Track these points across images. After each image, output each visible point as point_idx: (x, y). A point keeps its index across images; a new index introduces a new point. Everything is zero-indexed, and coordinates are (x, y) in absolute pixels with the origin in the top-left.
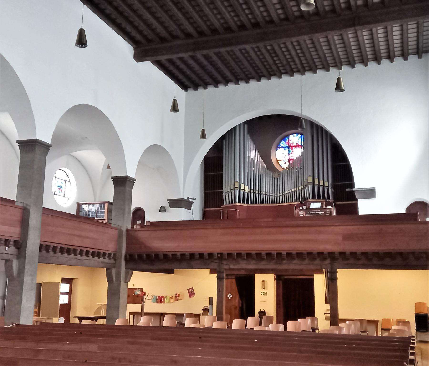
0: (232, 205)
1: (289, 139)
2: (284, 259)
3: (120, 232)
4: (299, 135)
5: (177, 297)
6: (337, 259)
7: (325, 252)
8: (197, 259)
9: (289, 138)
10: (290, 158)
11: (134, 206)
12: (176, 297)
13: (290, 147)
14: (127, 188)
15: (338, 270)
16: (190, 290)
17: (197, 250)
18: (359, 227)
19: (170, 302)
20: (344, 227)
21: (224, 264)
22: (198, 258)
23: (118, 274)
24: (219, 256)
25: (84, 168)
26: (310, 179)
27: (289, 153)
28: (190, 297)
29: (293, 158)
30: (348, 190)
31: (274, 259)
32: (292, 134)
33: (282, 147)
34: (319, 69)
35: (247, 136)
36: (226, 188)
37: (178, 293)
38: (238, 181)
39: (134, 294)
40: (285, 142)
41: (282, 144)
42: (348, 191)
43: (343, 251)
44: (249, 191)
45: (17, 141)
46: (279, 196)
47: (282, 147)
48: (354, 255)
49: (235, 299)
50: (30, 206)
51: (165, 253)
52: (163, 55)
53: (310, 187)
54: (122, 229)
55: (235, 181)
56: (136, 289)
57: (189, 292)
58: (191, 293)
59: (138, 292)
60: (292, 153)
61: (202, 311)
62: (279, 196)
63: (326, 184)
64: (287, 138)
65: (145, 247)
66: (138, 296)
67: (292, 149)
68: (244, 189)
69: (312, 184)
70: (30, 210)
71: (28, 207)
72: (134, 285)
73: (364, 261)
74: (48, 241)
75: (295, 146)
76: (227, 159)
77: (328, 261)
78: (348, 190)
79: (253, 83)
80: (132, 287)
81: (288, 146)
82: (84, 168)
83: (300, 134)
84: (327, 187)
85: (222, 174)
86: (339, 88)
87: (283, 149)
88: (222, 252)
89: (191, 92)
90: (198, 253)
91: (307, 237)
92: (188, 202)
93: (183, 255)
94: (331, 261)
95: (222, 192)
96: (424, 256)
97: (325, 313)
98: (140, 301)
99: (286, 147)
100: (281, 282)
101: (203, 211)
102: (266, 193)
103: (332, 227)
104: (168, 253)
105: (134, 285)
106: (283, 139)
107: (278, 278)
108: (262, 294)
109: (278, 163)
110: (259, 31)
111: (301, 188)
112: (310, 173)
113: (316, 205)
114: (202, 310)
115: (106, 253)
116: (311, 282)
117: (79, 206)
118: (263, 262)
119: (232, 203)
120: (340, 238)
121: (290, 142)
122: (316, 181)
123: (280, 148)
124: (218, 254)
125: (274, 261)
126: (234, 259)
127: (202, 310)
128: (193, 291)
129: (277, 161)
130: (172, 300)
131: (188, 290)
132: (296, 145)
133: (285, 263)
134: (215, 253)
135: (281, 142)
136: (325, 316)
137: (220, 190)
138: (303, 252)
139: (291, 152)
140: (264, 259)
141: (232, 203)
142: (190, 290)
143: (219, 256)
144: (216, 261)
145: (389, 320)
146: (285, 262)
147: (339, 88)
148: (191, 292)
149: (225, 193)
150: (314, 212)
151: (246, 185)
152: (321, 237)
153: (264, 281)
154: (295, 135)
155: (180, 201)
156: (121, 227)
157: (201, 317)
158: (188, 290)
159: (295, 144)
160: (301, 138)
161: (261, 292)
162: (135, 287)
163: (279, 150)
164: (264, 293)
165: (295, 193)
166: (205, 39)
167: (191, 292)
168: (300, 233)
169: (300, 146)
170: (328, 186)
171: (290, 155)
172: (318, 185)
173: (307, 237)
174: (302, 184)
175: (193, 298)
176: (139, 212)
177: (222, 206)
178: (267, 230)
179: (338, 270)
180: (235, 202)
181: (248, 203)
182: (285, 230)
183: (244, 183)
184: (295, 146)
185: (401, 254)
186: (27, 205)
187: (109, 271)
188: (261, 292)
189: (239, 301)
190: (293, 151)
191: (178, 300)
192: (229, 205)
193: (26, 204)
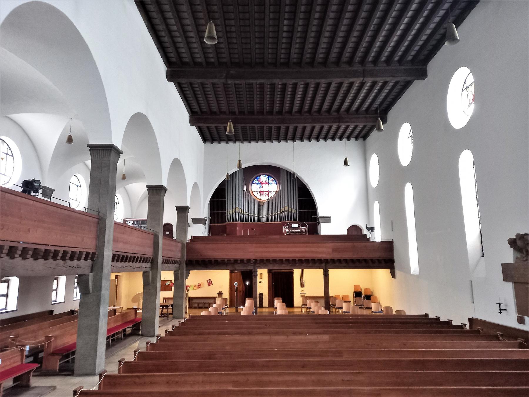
0: (230, 223)
1: (260, 178)
2: (297, 263)
3: (183, 244)
4: (267, 176)
5: (199, 286)
6: (329, 263)
7: (323, 259)
8: (239, 264)
9: (260, 177)
10: (261, 191)
11: (165, 222)
12: (198, 286)
13: (261, 183)
14: (187, 214)
15: (329, 269)
16: (209, 281)
17: (239, 257)
18: (342, 244)
19: (193, 289)
20: (333, 244)
21: (257, 266)
22: (239, 263)
23: (182, 274)
24: (254, 261)
25: (127, 192)
26: (286, 208)
27: (260, 187)
28: (209, 285)
29: (263, 191)
30: (313, 216)
31: (290, 263)
32: (262, 175)
33: (256, 183)
34: (298, 139)
35: (243, 176)
36: (229, 212)
37: (199, 283)
38: (238, 206)
39: (165, 285)
40: (258, 180)
41: (256, 181)
42: (313, 218)
43: (333, 259)
44: (244, 213)
45: (146, 186)
46: (264, 217)
47: (256, 183)
48: (339, 261)
49: (240, 286)
50: (159, 233)
51: (215, 259)
52: (213, 123)
53: (286, 213)
54: (184, 243)
55: (236, 207)
56: (167, 281)
57: (208, 282)
58: (210, 283)
59: (168, 283)
60: (262, 187)
61: (218, 295)
62: (264, 217)
63: (295, 212)
64: (259, 177)
65: (201, 255)
66: (168, 285)
67: (262, 185)
68: (241, 212)
69: (288, 211)
70: (159, 236)
71: (157, 234)
72: (165, 278)
73: (345, 264)
74: (121, 251)
75: (264, 183)
76: (229, 190)
77: (323, 265)
78: (313, 216)
79: (253, 143)
80: (164, 279)
81: (259, 182)
82: (127, 192)
83: (267, 175)
84: (291, 212)
85: (225, 200)
86: (346, 164)
87: (256, 184)
88: (256, 259)
89: (208, 144)
90: (239, 260)
91: (313, 249)
92: (204, 219)
93: (229, 260)
94: (325, 264)
95: (225, 213)
96: (377, 261)
97: (300, 293)
98: (170, 289)
99: (258, 183)
100: (271, 274)
101: (209, 225)
102: (255, 215)
103: (326, 244)
104: (219, 260)
105: (165, 278)
106: (256, 178)
107: (269, 272)
108: (260, 282)
109: (253, 193)
110: (280, 117)
111: (279, 213)
112: (286, 204)
113: (295, 226)
114: (218, 294)
115: (252, 270)
116: (292, 274)
117: (125, 221)
118: (283, 265)
119: (233, 221)
120: (331, 250)
121: (261, 180)
122: (290, 210)
123: (254, 183)
124: (253, 260)
125: (290, 264)
126: (264, 263)
127: (218, 294)
128: (211, 281)
129: (252, 192)
130: (195, 288)
131: (207, 281)
132: (265, 182)
133: (297, 266)
134: (252, 259)
135: (255, 180)
136: (300, 295)
137: (224, 211)
138: (309, 259)
139: (261, 186)
140: (284, 263)
141: (233, 221)
142: (209, 281)
143: (254, 261)
144: (252, 264)
145: (340, 295)
146: (297, 265)
147: (346, 164)
148: (210, 282)
149: (228, 214)
150: (294, 230)
151: (242, 209)
152: (320, 250)
153: (261, 274)
154: (264, 176)
155: (201, 220)
156: (183, 241)
157: (217, 298)
158: (207, 281)
159: (264, 182)
160: (268, 178)
161: (259, 281)
162: (166, 279)
163: (253, 184)
164: (261, 281)
165: (277, 215)
166: (242, 116)
167: (210, 282)
168: (306, 247)
169: (268, 183)
170: (297, 213)
171: (261, 189)
172: (291, 212)
173: (313, 249)
174: (280, 211)
175: (211, 286)
176: (168, 226)
177: (225, 223)
178: (286, 245)
179: (329, 269)
180: (236, 221)
181: (243, 221)
182: (297, 245)
183: (241, 208)
184: (264, 183)
185: (366, 261)
186: (157, 232)
187: (176, 272)
188: (259, 281)
189: (242, 287)
190: (262, 186)
191: (199, 288)
192: (228, 223)
193: (155, 231)
